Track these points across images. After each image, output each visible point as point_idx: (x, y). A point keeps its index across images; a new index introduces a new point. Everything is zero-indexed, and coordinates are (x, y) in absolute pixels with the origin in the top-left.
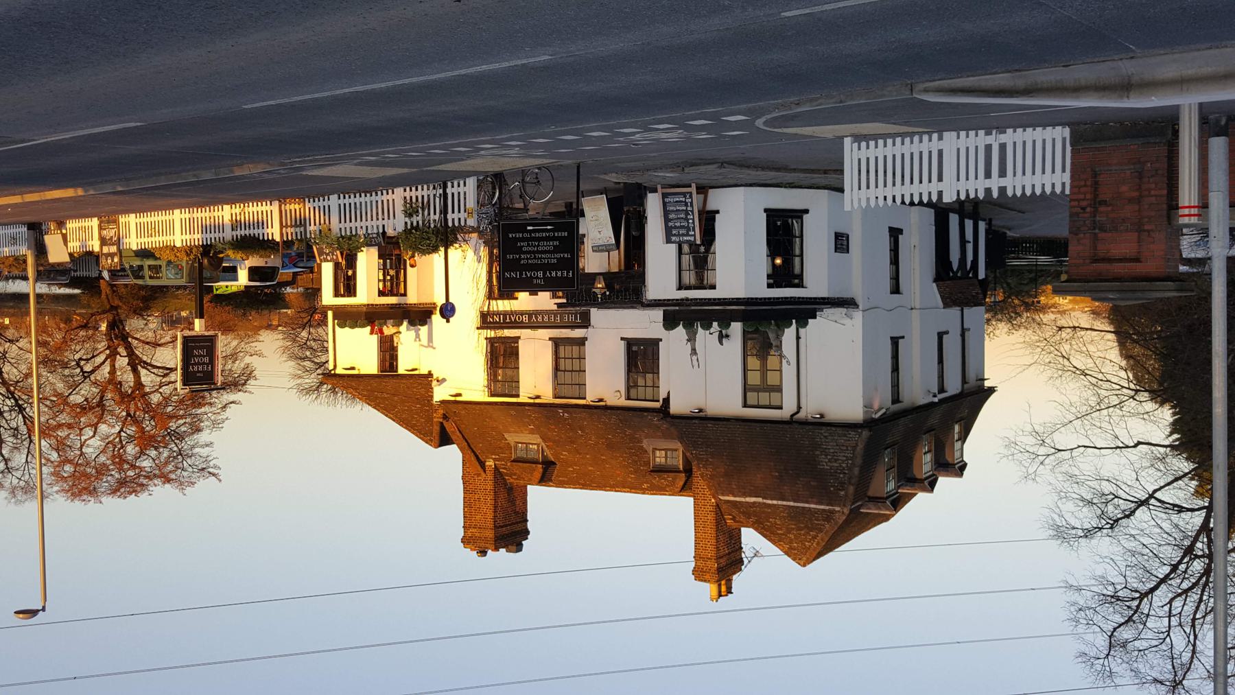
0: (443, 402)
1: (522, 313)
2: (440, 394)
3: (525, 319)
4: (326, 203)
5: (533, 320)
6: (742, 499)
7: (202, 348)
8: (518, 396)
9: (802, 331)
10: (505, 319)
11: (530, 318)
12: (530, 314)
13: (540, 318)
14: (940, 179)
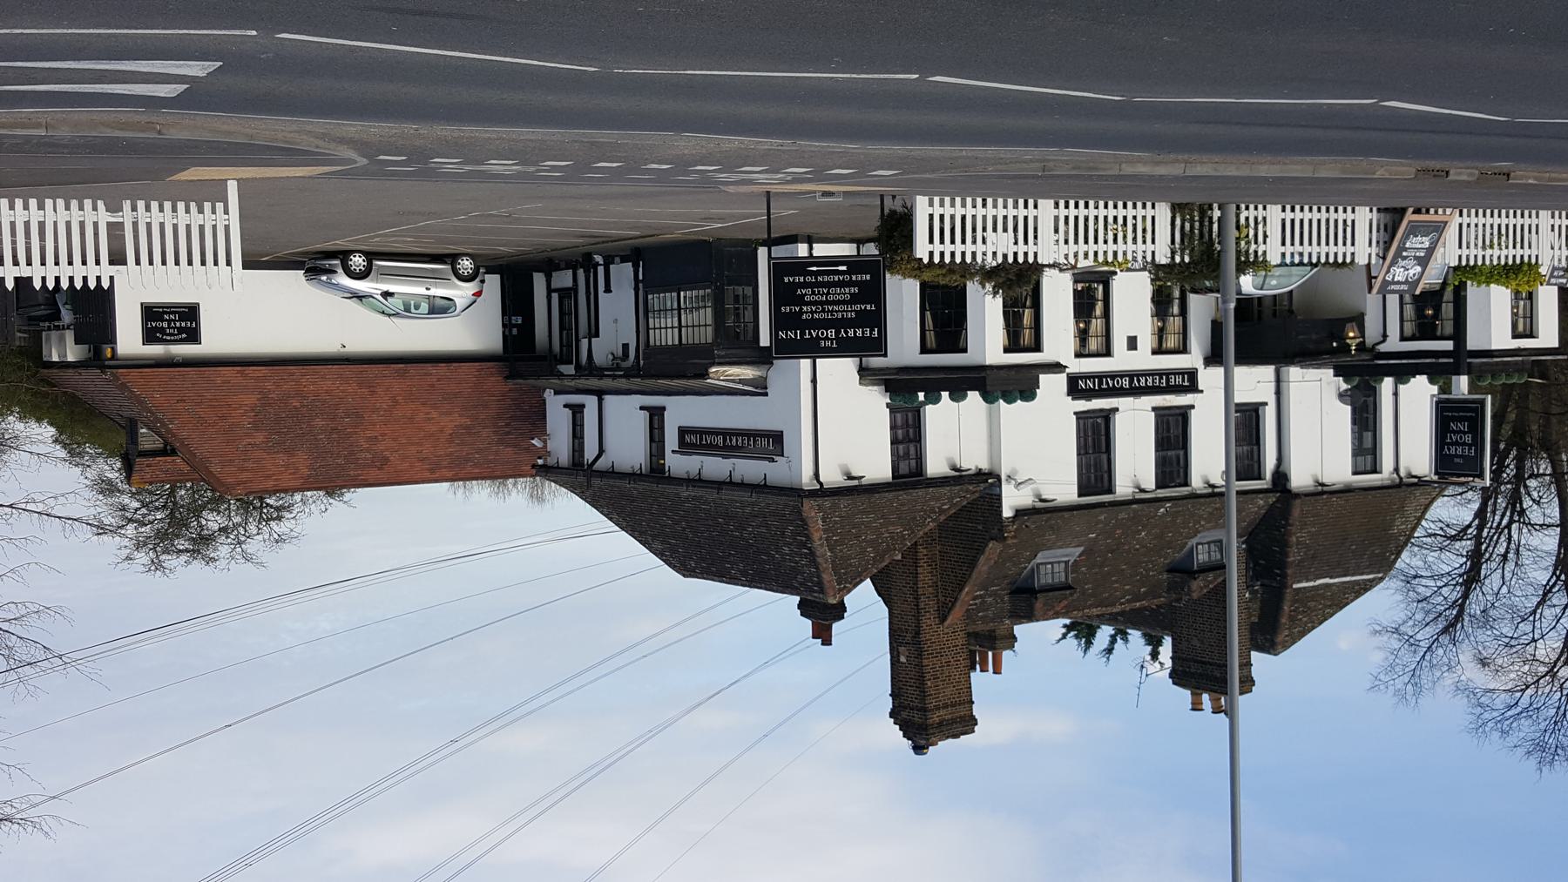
0: (1020, 513)
1: (1122, 375)
2: (1012, 500)
3: (1126, 383)
4: (1149, 212)
5: (1135, 385)
6: (1311, 584)
7: (1461, 419)
8: (1110, 490)
9: (1401, 387)
10: (1100, 383)
11: (1131, 382)
12: (1132, 375)
13: (1143, 380)
14: (931, 216)
